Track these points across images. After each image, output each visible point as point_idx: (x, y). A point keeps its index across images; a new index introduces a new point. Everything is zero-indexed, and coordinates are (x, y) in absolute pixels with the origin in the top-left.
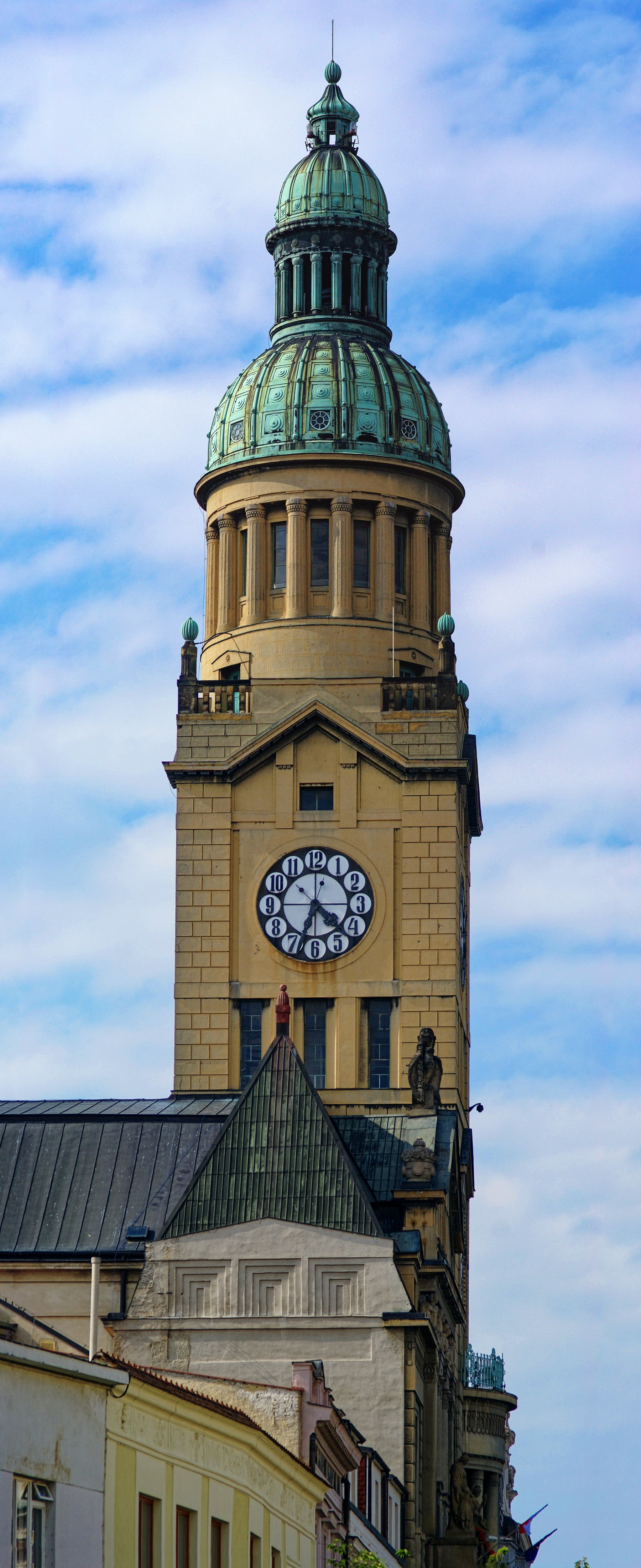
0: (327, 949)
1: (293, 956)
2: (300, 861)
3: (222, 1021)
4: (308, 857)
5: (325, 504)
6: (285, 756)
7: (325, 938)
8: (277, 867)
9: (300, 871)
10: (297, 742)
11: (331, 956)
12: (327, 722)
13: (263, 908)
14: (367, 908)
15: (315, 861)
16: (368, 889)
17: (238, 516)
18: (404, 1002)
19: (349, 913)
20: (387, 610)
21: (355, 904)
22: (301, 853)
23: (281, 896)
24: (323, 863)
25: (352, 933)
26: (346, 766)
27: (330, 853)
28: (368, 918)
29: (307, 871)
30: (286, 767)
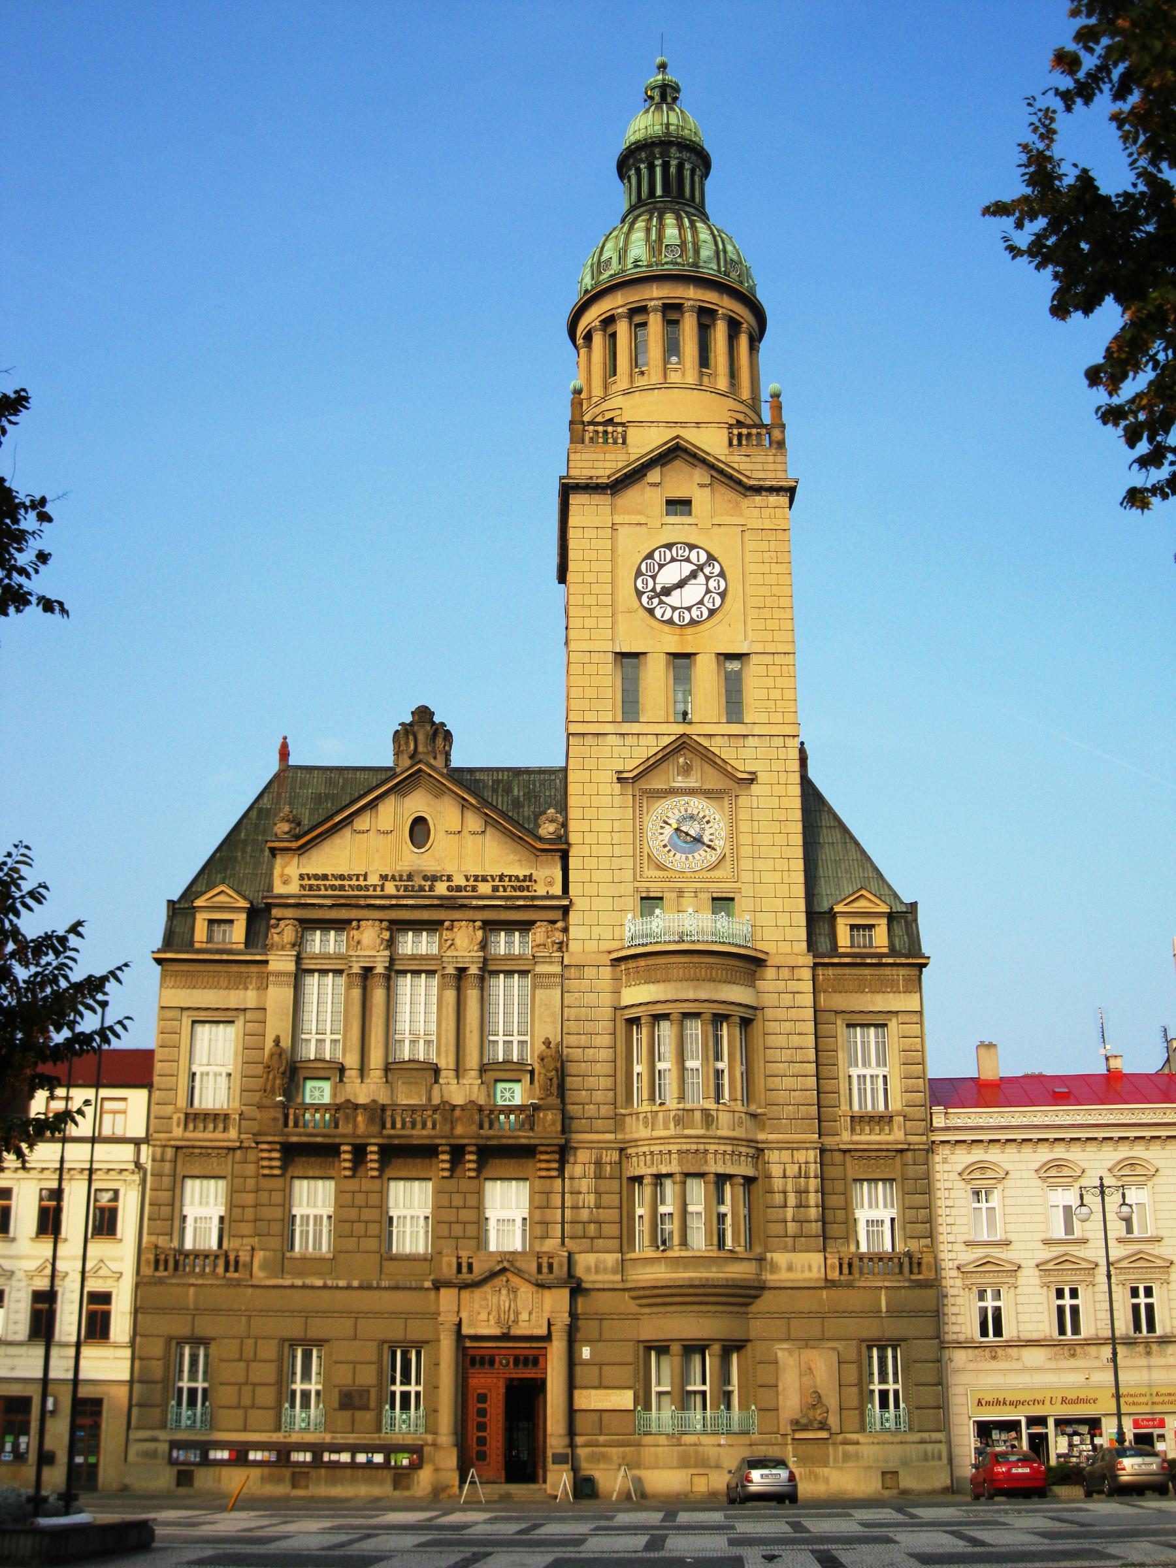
0: (692, 618)
1: (664, 621)
2: (668, 552)
3: (609, 668)
4: (674, 549)
5: (678, 307)
6: (654, 476)
7: (689, 609)
8: (650, 556)
9: (668, 558)
10: (662, 465)
11: (693, 622)
12: (685, 450)
13: (640, 585)
14: (722, 588)
15: (680, 552)
16: (722, 574)
17: (609, 321)
18: (754, 659)
19: (708, 591)
20: (722, 383)
21: (712, 584)
22: (669, 546)
23: (654, 577)
24: (686, 554)
25: (710, 606)
26: (701, 486)
27: (692, 547)
28: (723, 595)
29: (673, 560)
30: (656, 485)
